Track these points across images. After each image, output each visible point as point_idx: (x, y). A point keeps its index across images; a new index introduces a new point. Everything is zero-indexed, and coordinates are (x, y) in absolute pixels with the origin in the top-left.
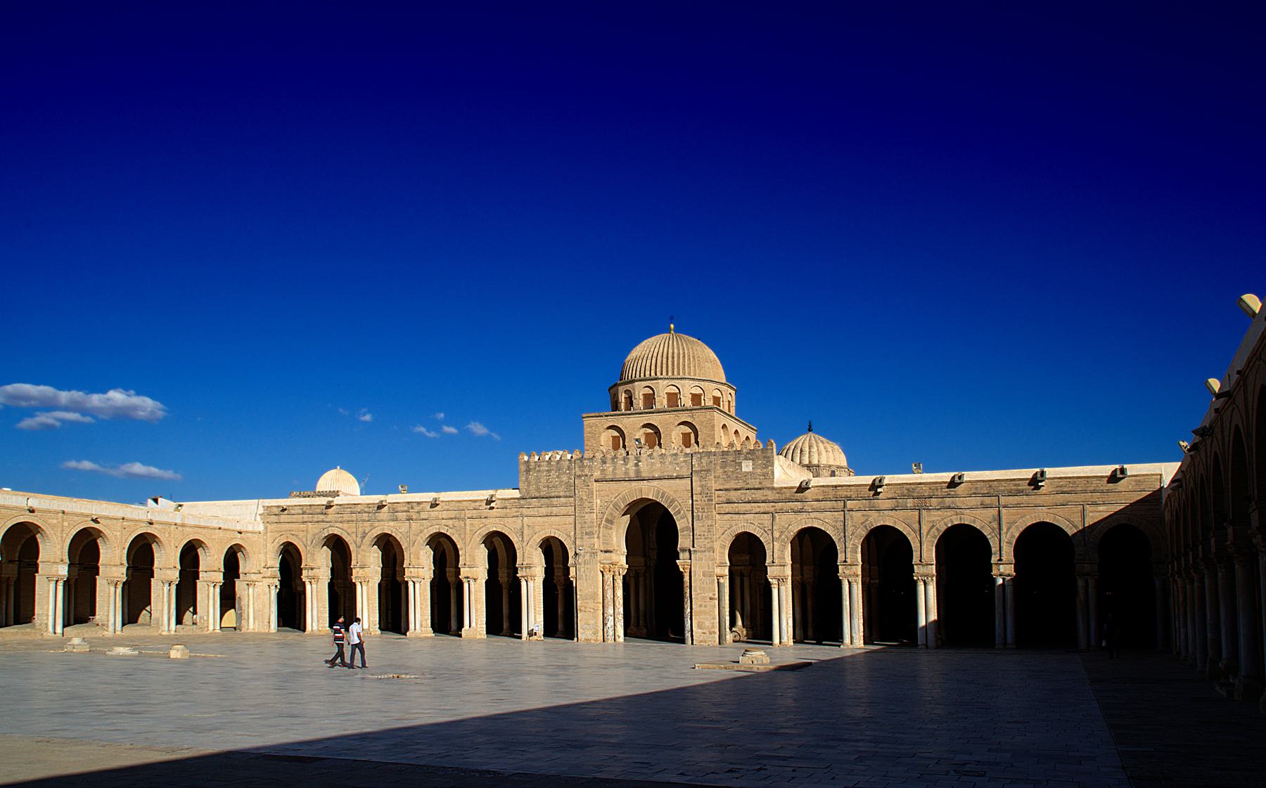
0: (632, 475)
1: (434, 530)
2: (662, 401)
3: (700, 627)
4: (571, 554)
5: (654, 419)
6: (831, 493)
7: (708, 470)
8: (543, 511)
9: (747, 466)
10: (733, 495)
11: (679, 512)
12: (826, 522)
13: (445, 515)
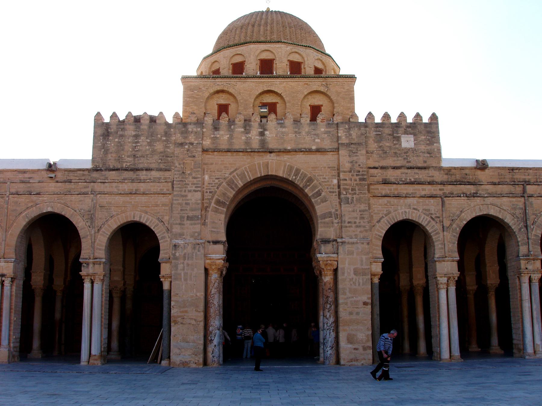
0: (255, 144)
2: (281, 67)
3: (350, 340)
6: (508, 177)
8: (127, 187)
9: (407, 142)
10: (391, 175)
11: (319, 194)
12: (503, 209)
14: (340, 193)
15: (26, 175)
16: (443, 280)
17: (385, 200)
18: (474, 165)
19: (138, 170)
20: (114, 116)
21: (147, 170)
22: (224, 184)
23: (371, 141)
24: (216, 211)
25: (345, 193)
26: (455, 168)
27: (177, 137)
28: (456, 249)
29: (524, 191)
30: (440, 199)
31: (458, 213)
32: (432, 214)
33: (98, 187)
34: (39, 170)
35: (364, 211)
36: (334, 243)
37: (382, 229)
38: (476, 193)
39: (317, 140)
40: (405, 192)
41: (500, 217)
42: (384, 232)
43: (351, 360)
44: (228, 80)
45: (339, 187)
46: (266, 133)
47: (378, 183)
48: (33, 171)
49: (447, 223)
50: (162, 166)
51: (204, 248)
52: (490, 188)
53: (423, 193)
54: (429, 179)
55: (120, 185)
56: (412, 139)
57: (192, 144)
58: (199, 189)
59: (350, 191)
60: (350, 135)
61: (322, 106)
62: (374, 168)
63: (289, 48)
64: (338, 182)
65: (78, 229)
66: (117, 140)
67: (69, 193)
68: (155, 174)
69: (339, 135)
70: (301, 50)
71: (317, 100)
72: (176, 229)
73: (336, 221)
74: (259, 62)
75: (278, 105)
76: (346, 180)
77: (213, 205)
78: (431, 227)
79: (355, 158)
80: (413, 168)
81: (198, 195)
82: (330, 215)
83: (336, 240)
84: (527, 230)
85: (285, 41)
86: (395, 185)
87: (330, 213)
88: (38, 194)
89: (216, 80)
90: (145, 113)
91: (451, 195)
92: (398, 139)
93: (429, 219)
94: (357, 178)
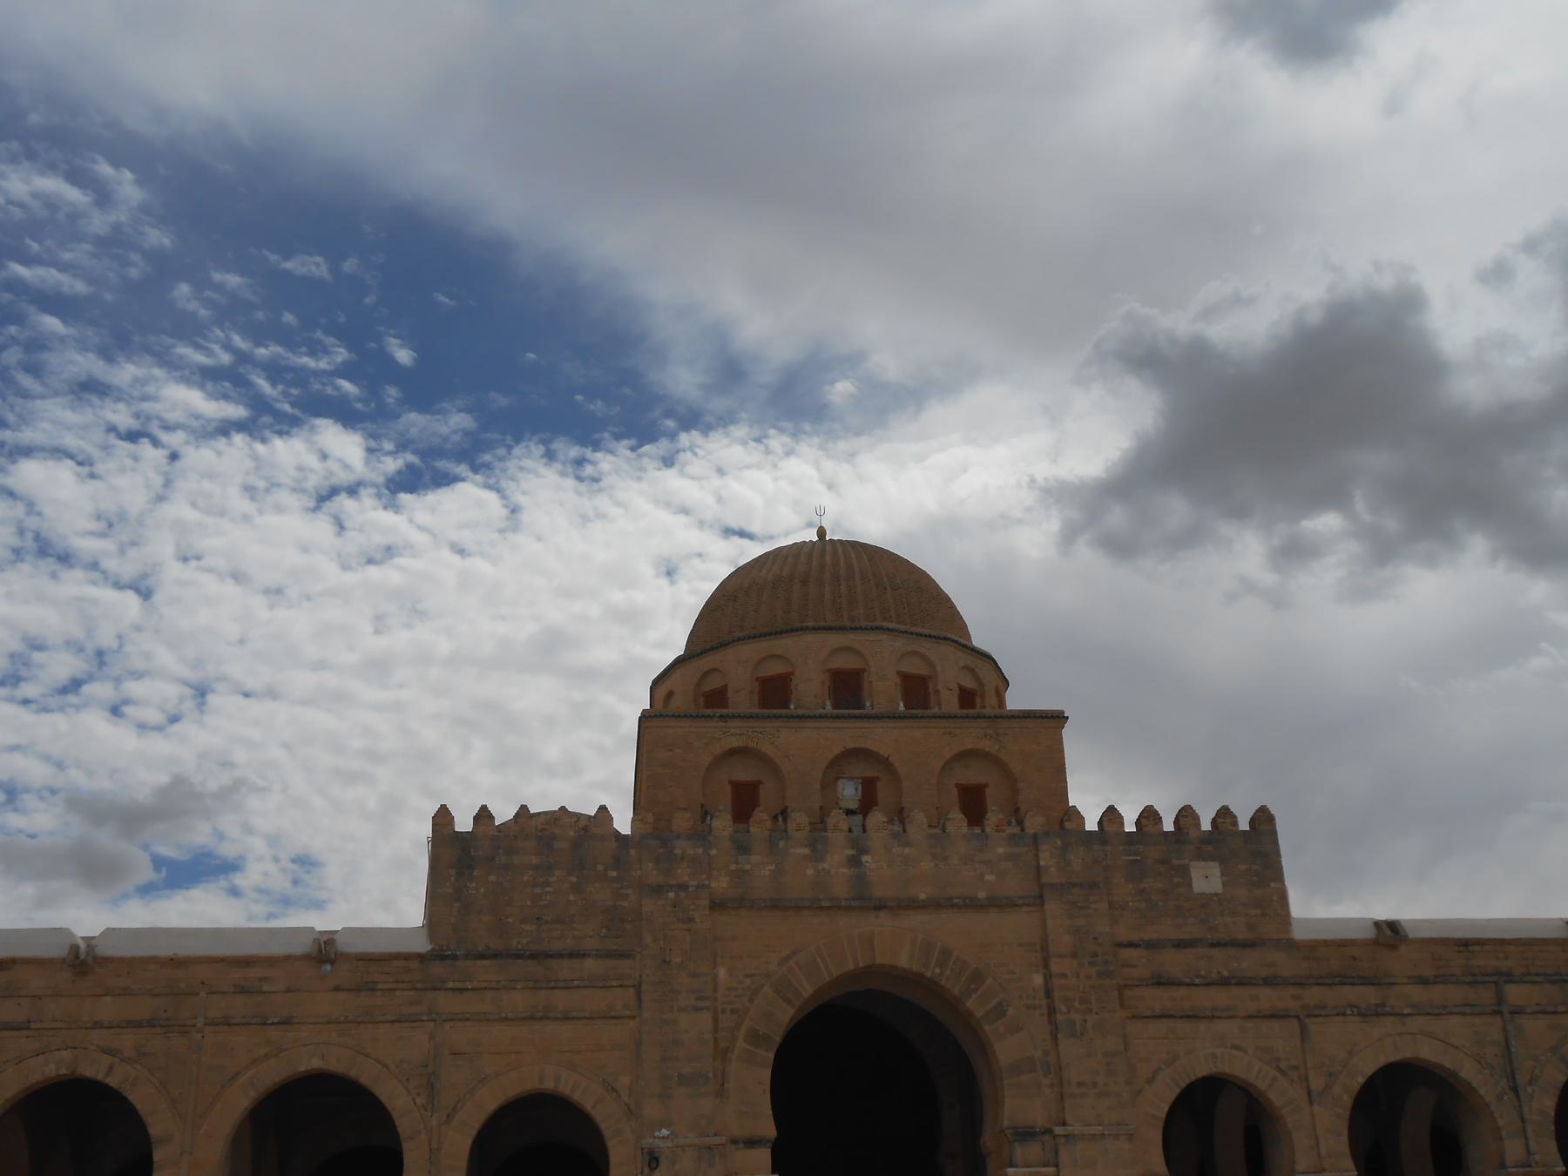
2: (883, 689)
5: (880, 738)
9: (1206, 879)
10: (1174, 962)
12: (1453, 1044)
14: (1052, 1011)
15: (254, 973)
18: (1370, 934)
19: (549, 956)
20: (483, 815)
21: (571, 955)
22: (767, 989)
25: (1064, 1009)
28: (1347, 1151)
29: (1500, 1000)
32: (1278, 1060)
34: (288, 958)
36: (1047, 1137)
38: (1383, 1005)
39: (989, 877)
41: (1447, 1065)
42: (1166, 1108)
45: (1048, 993)
46: (865, 858)
48: (271, 961)
49: (1317, 1083)
52: (1417, 993)
56: (1217, 871)
57: (683, 887)
58: (707, 1004)
59: (1076, 1004)
61: (986, 785)
62: (1131, 945)
63: (900, 644)
64: (1046, 982)
65: (395, 1114)
66: (492, 878)
68: (592, 966)
69: (1042, 863)
70: (926, 647)
71: (972, 774)
73: (1046, 1081)
75: (879, 785)
76: (1064, 976)
77: (741, 1043)
78: (1280, 1094)
80: (1225, 945)
83: (1049, 1131)
84: (1518, 1096)
86: (1182, 991)
88: (286, 1022)
89: (730, 724)
90: (563, 809)
92: (1184, 872)
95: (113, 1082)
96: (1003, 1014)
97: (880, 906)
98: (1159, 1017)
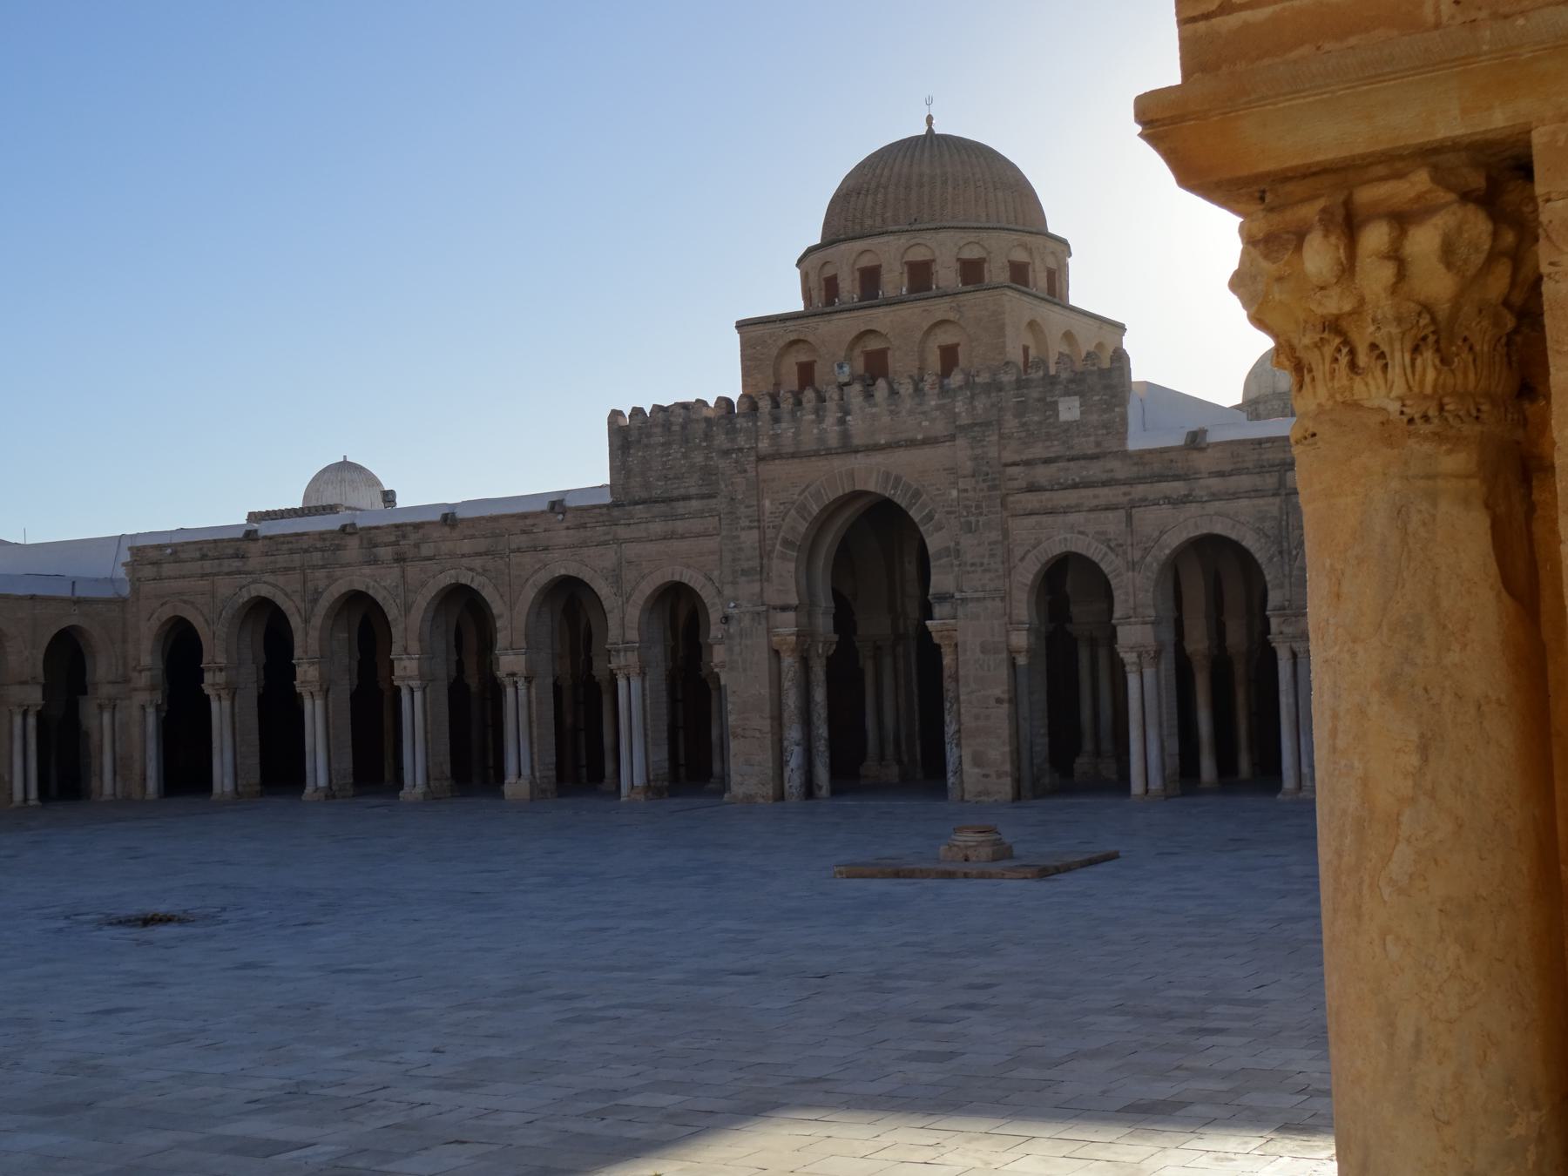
1: (446, 579)
2: (894, 281)
3: (978, 761)
4: (715, 616)
7: (988, 424)
8: (657, 527)
9: (1069, 409)
10: (1042, 474)
11: (930, 517)
13: (466, 546)
15: (529, 522)
16: (1129, 658)
17: (1033, 520)
19: (671, 500)
22: (793, 512)
23: (1009, 417)
24: (783, 557)
26: (1150, 451)
27: (721, 440)
30: (1122, 512)
31: (1156, 534)
33: (622, 532)
35: (996, 543)
37: (1028, 572)
38: (1187, 496)
39: (925, 424)
40: (1064, 503)
42: (1031, 577)
43: (979, 794)
44: (804, 321)
47: (1020, 491)
50: (705, 491)
51: (767, 618)
52: (1216, 483)
53: (1095, 502)
54: (1104, 477)
55: (651, 526)
56: (1077, 404)
57: (741, 450)
60: (974, 408)
63: (903, 240)
67: (584, 544)
68: (695, 504)
71: (945, 337)
72: (728, 591)
74: (857, 274)
76: (966, 491)
79: (979, 451)
81: (755, 534)
82: (946, 552)
85: (895, 228)
86: (1047, 494)
87: (947, 549)
88: (546, 549)
91: (1144, 502)
93: (1104, 549)
94: (984, 486)
95: (474, 586)
96: (932, 519)
97: (857, 452)
98: (1031, 514)
